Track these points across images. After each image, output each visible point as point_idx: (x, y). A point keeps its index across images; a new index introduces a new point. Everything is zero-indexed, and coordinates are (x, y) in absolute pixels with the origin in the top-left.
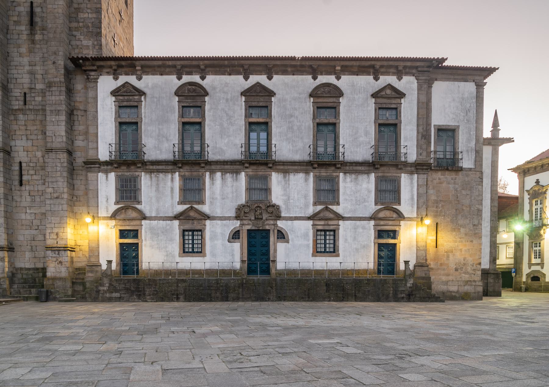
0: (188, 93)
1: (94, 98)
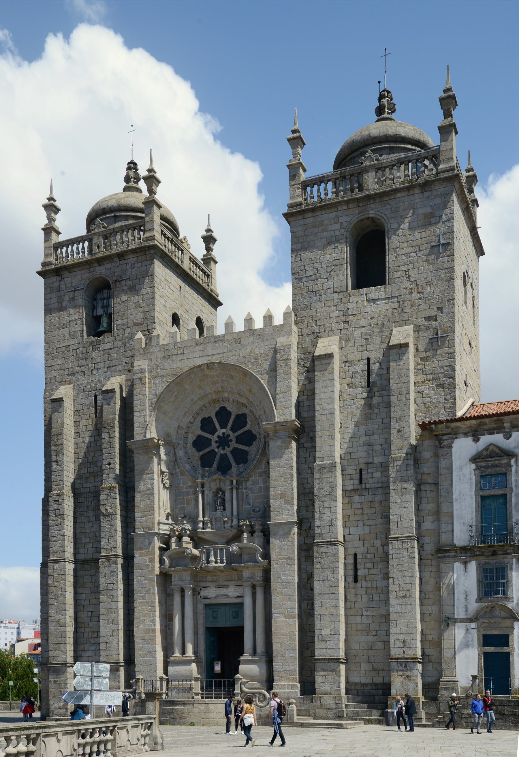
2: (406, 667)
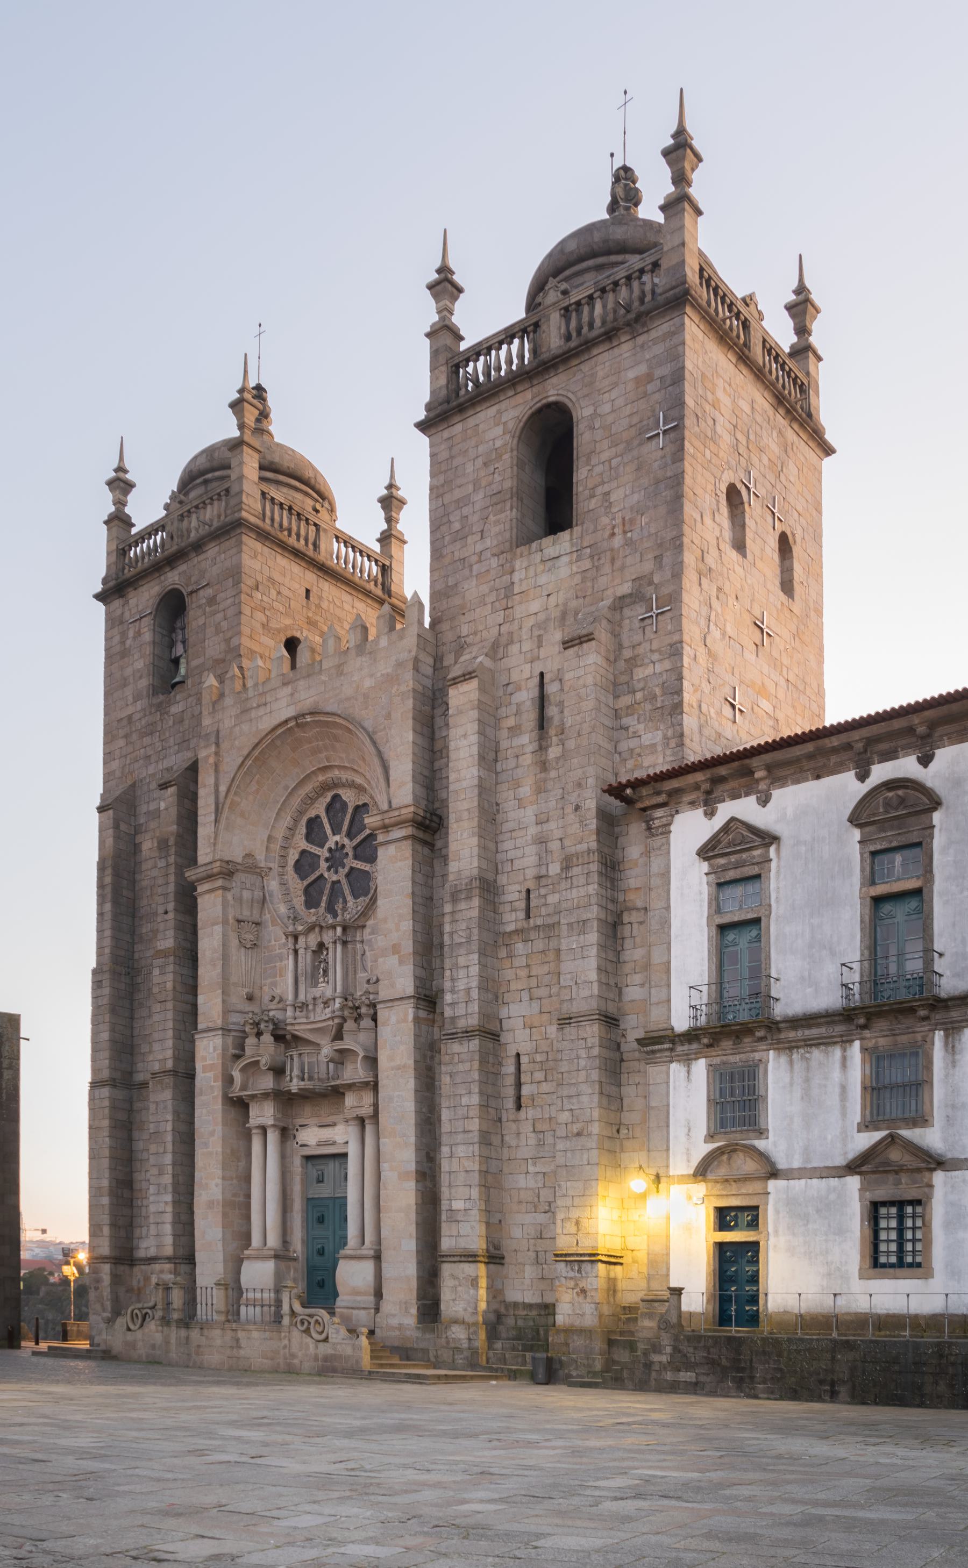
0: (886, 812)
1: (663, 874)
2: (579, 1271)
